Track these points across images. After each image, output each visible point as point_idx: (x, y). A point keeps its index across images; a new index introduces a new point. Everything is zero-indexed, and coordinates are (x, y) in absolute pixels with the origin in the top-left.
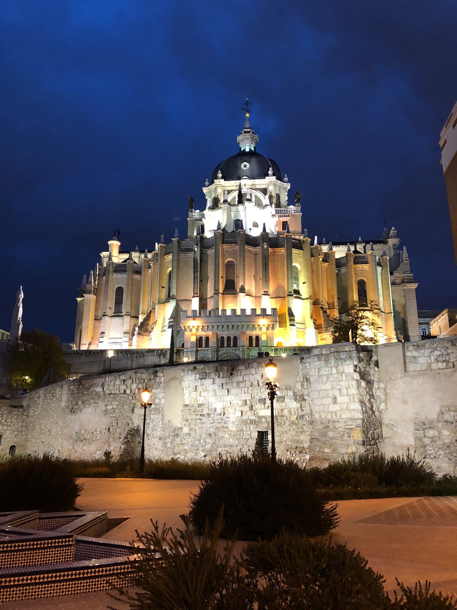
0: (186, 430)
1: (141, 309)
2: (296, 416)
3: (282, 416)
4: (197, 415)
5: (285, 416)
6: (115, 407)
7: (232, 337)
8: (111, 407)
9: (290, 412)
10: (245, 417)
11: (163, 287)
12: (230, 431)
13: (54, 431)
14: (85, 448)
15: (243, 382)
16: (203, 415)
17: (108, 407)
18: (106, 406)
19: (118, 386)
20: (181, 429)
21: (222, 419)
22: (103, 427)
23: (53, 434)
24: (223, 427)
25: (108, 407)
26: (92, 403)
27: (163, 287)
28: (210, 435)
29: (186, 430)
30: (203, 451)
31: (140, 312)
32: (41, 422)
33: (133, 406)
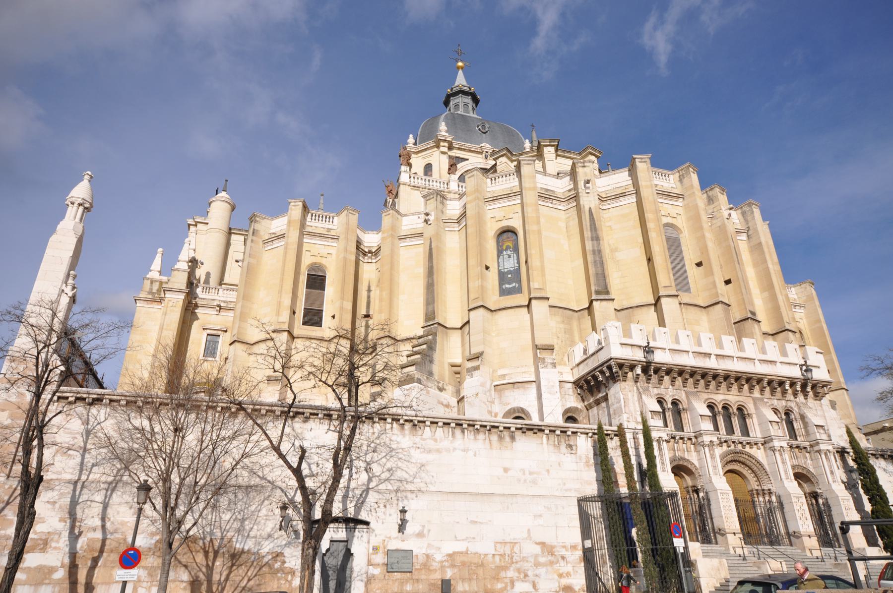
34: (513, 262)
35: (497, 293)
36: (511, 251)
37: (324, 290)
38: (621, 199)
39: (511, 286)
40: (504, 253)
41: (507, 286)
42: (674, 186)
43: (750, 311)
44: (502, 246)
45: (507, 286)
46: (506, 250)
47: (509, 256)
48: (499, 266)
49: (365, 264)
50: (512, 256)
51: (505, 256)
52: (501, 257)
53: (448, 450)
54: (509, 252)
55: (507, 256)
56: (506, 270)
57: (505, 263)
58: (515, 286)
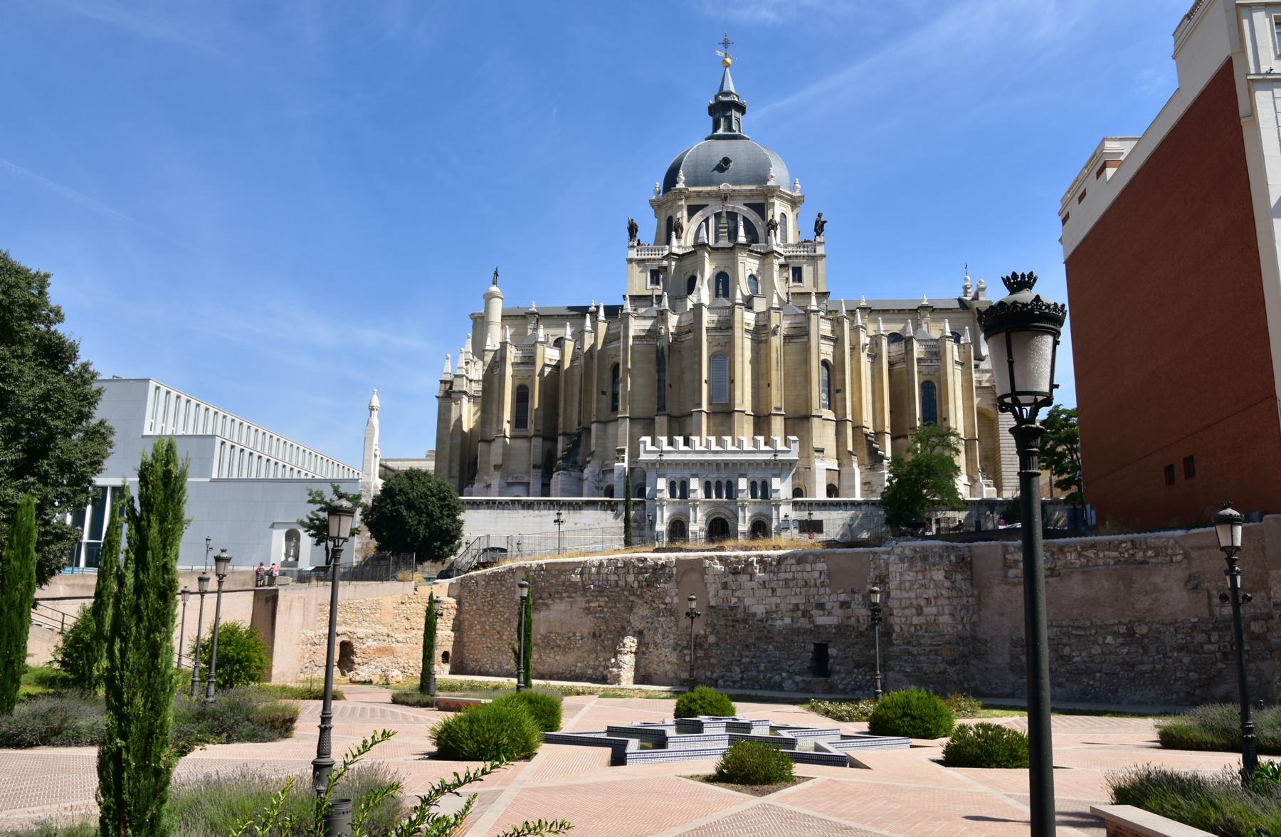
0: (712, 639)
1: (561, 426)
2: (865, 626)
3: (847, 626)
4: (728, 620)
5: (850, 626)
6: (602, 604)
7: (724, 482)
8: (597, 604)
9: (858, 620)
10: (796, 626)
11: (604, 393)
12: (777, 642)
13: (506, 633)
14: (558, 658)
15: (794, 579)
16: (737, 621)
17: (592, 604)
18: (588, 602)
19: (605, 576)
20: (706, 637)
21: (764, 627)
22: (585, 631)
23: (504, 637)
24: (766, 637)
25: (592, 604)
26: (564, 598)
27: (604, 393)
28: (747, 646)
29: (712, 639)
30: (738, 666)
31: (560, 431)
32: (483, 619)
33: (630, 604)
35: (610, 409)
53: (546, 516)
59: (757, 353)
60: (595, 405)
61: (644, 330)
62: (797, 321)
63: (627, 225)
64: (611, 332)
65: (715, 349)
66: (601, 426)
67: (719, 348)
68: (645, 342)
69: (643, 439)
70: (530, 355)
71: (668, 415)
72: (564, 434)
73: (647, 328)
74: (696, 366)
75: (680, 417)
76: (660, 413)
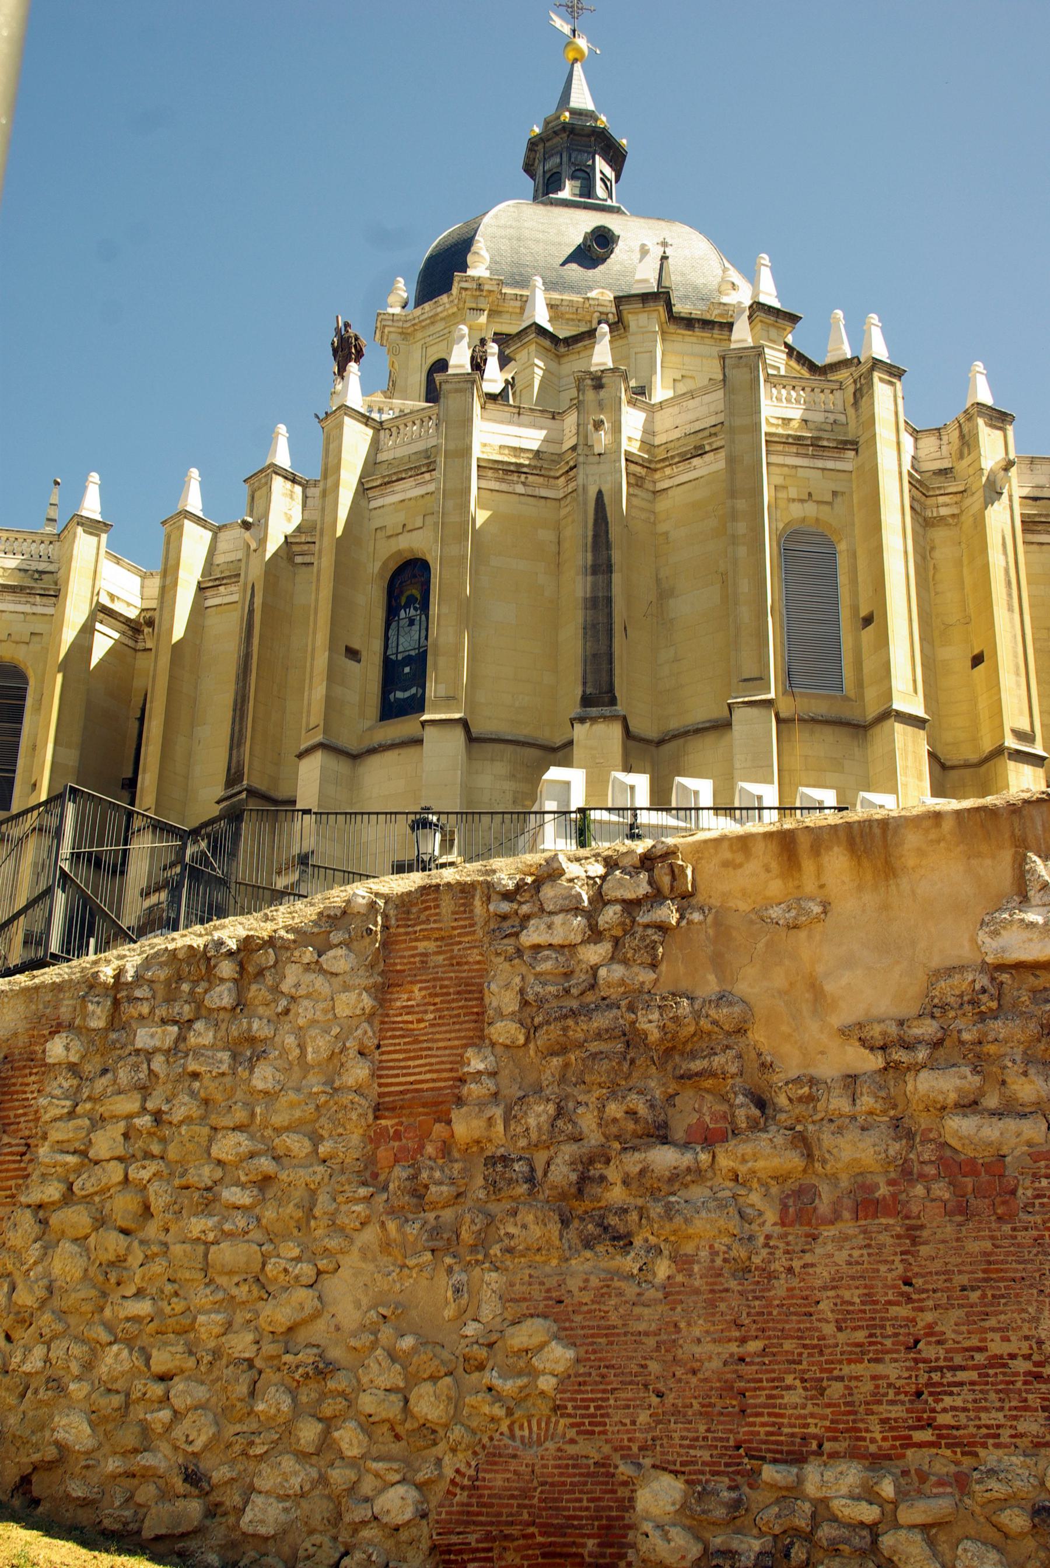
11: (353, 654)
27: (353, 654)
34: (416, 637)
36: (416, 609)
37: (20, 720)
38: (696, 461)
39: (407, 694)
40: (402, 614)
41: (400, 695)
42: (842, 418)
43: (1013, 731)
44: (399, 597)
45: (400, 695)
46: (407, 606)
47: (412, 622)
48: (386, 647)
49: (139, 654)
50: (417, 622)
51: (402, 623)
52: (394, 625)
54: (412, 612)
55: (405, 622)
56: (400, 657)
57: (402, 640)
58: (414, 695)
59: (924, 558)
60: (319, 691)
61: (518, 451)
62: (1042, 480)
63: (332, 337)
64: (381, 457)
65: (797, 511)
66: (339, 766)
67: (810, 510)
68: (520, 489)
69: (554, 773)
70: (42, 567)
71: (624, 720)
72: (160, 828)
73: (535, 446)
74: (742, 551)
75: (660, 742)
76: (594, 711)
